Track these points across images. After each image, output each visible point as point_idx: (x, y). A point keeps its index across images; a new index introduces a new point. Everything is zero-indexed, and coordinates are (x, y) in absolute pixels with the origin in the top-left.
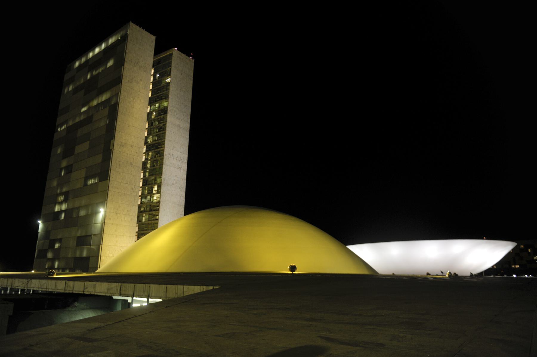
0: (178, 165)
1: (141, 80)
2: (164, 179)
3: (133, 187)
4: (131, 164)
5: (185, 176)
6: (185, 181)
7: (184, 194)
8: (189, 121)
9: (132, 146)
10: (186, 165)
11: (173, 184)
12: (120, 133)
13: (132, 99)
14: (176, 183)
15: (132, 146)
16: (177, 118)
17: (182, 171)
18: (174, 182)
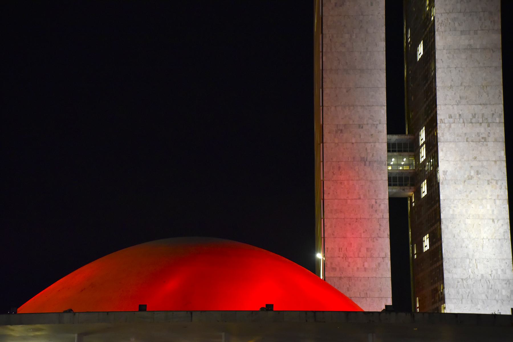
0: (478, 134)
2: (445, 172)
3: (373, 202)
4: (364, 160)
5: (503, 154)
6: (504, 164)
7: (504, 193)
8: (498, 26)
10: (503, 128)
11: (470, 178)
12: (333, 108)
13: (347, 36)
14: (478, 173)
16: (462, 32)
17: (491, 144)
18: (473, 173)
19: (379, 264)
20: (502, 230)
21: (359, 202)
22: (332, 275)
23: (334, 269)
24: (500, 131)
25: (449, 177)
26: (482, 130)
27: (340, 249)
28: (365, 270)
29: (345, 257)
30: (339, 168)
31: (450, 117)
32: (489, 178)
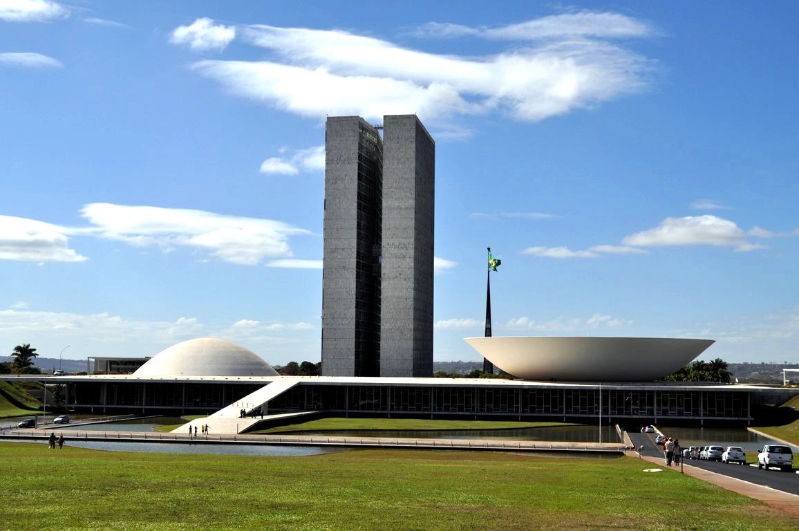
1: (346, 175)
2: (384, 274)
5: (413, 264)
8: (413, 196)
9: (343, 249)
11: (396, 277)
14: (400, 274)
15: (343, 249)
16: (396, 199)
17: (407, 259)
18: (398, 275)
19: (350, 322)
20: (409, 304)
21: (341, 290)
22: (326, 327)
23: (327, 324)
24: (412, 252)
25: (386, 277)
26: (403, 251)
27: (331, 314)
28: (343, 325)
29: (333, 318)
30: (332, 272)
31: (388, 244)
32: (405, 277)
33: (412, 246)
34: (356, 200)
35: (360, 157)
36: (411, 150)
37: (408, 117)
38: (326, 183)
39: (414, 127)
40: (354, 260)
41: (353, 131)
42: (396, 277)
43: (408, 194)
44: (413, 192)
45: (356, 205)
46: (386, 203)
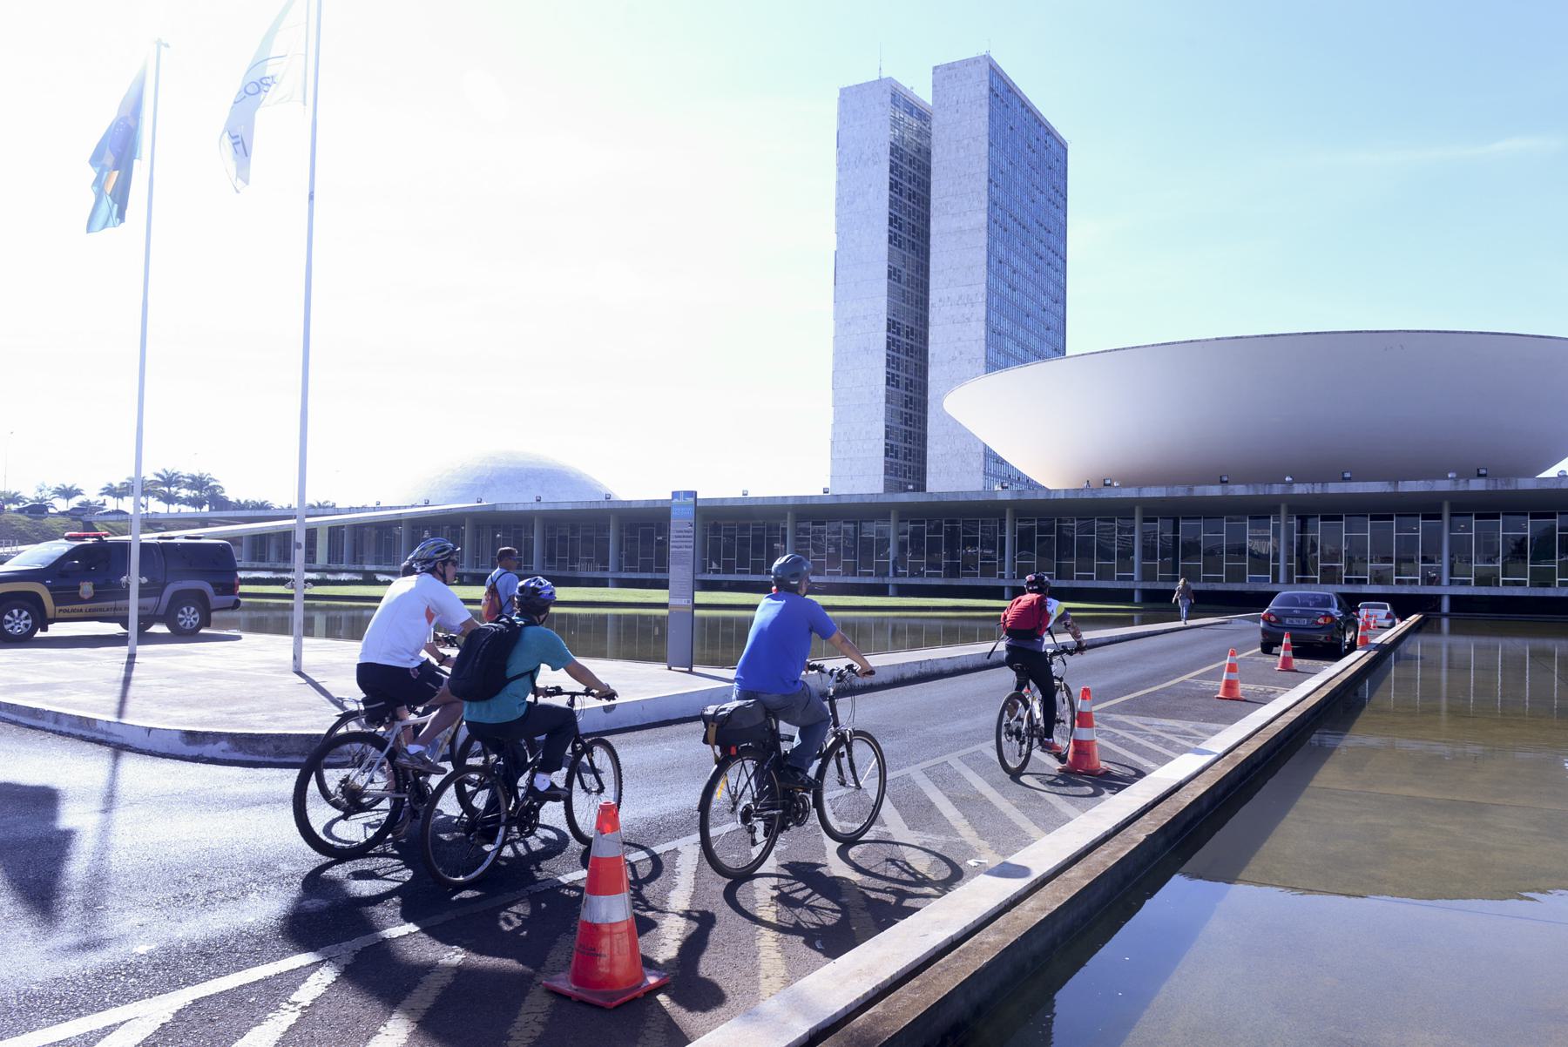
9: (865, 317)
11: (954, 359)
15: (865, 317)
24: (981, 311)
26: (966, 310)
33: (982, 299)
34: (886, 226)
35: (894, 150)
36: (978, 121)
37: (976, 61)
38: (838, 205)
39: (986, 78)
40: (882, 335)
41: (882, 104)
42: (954, 359)
43: (976, 204)
44: (985, 197)
45: (886, 236)
46: (938, 225)
